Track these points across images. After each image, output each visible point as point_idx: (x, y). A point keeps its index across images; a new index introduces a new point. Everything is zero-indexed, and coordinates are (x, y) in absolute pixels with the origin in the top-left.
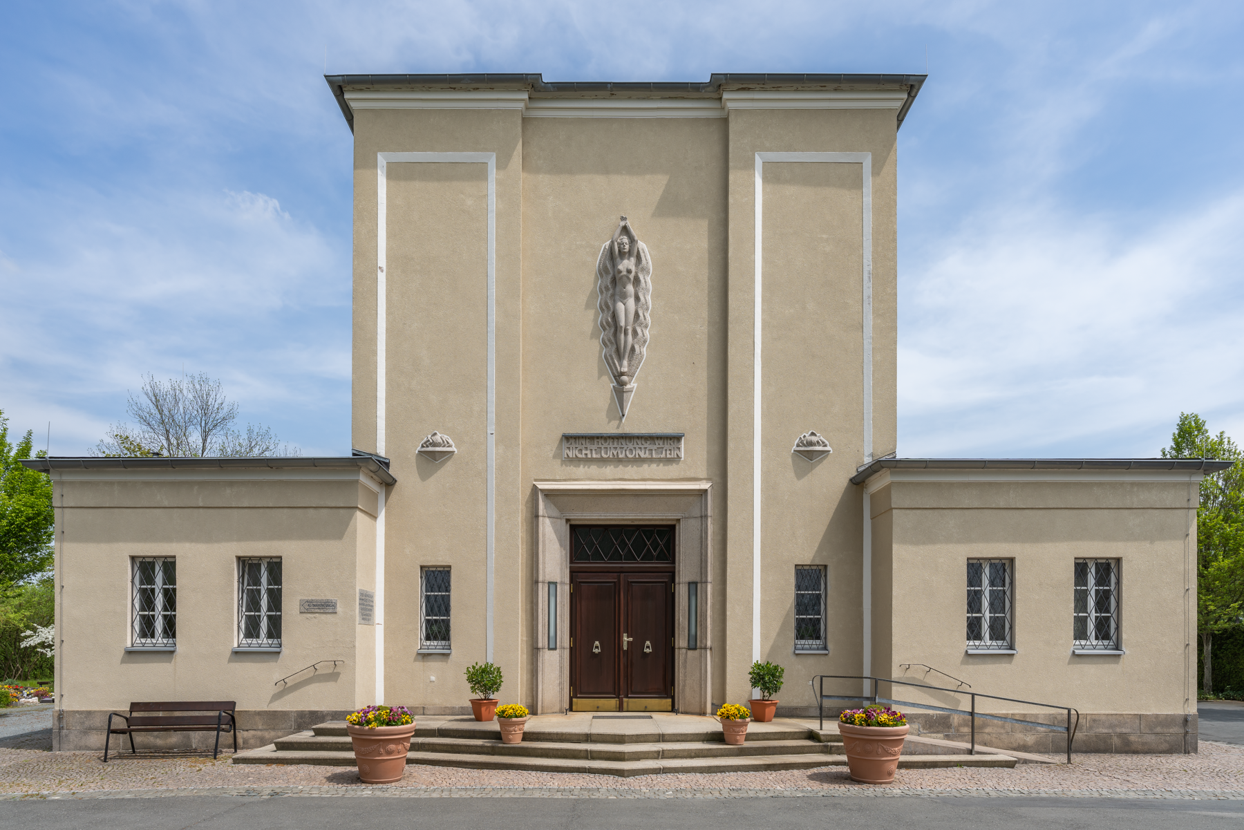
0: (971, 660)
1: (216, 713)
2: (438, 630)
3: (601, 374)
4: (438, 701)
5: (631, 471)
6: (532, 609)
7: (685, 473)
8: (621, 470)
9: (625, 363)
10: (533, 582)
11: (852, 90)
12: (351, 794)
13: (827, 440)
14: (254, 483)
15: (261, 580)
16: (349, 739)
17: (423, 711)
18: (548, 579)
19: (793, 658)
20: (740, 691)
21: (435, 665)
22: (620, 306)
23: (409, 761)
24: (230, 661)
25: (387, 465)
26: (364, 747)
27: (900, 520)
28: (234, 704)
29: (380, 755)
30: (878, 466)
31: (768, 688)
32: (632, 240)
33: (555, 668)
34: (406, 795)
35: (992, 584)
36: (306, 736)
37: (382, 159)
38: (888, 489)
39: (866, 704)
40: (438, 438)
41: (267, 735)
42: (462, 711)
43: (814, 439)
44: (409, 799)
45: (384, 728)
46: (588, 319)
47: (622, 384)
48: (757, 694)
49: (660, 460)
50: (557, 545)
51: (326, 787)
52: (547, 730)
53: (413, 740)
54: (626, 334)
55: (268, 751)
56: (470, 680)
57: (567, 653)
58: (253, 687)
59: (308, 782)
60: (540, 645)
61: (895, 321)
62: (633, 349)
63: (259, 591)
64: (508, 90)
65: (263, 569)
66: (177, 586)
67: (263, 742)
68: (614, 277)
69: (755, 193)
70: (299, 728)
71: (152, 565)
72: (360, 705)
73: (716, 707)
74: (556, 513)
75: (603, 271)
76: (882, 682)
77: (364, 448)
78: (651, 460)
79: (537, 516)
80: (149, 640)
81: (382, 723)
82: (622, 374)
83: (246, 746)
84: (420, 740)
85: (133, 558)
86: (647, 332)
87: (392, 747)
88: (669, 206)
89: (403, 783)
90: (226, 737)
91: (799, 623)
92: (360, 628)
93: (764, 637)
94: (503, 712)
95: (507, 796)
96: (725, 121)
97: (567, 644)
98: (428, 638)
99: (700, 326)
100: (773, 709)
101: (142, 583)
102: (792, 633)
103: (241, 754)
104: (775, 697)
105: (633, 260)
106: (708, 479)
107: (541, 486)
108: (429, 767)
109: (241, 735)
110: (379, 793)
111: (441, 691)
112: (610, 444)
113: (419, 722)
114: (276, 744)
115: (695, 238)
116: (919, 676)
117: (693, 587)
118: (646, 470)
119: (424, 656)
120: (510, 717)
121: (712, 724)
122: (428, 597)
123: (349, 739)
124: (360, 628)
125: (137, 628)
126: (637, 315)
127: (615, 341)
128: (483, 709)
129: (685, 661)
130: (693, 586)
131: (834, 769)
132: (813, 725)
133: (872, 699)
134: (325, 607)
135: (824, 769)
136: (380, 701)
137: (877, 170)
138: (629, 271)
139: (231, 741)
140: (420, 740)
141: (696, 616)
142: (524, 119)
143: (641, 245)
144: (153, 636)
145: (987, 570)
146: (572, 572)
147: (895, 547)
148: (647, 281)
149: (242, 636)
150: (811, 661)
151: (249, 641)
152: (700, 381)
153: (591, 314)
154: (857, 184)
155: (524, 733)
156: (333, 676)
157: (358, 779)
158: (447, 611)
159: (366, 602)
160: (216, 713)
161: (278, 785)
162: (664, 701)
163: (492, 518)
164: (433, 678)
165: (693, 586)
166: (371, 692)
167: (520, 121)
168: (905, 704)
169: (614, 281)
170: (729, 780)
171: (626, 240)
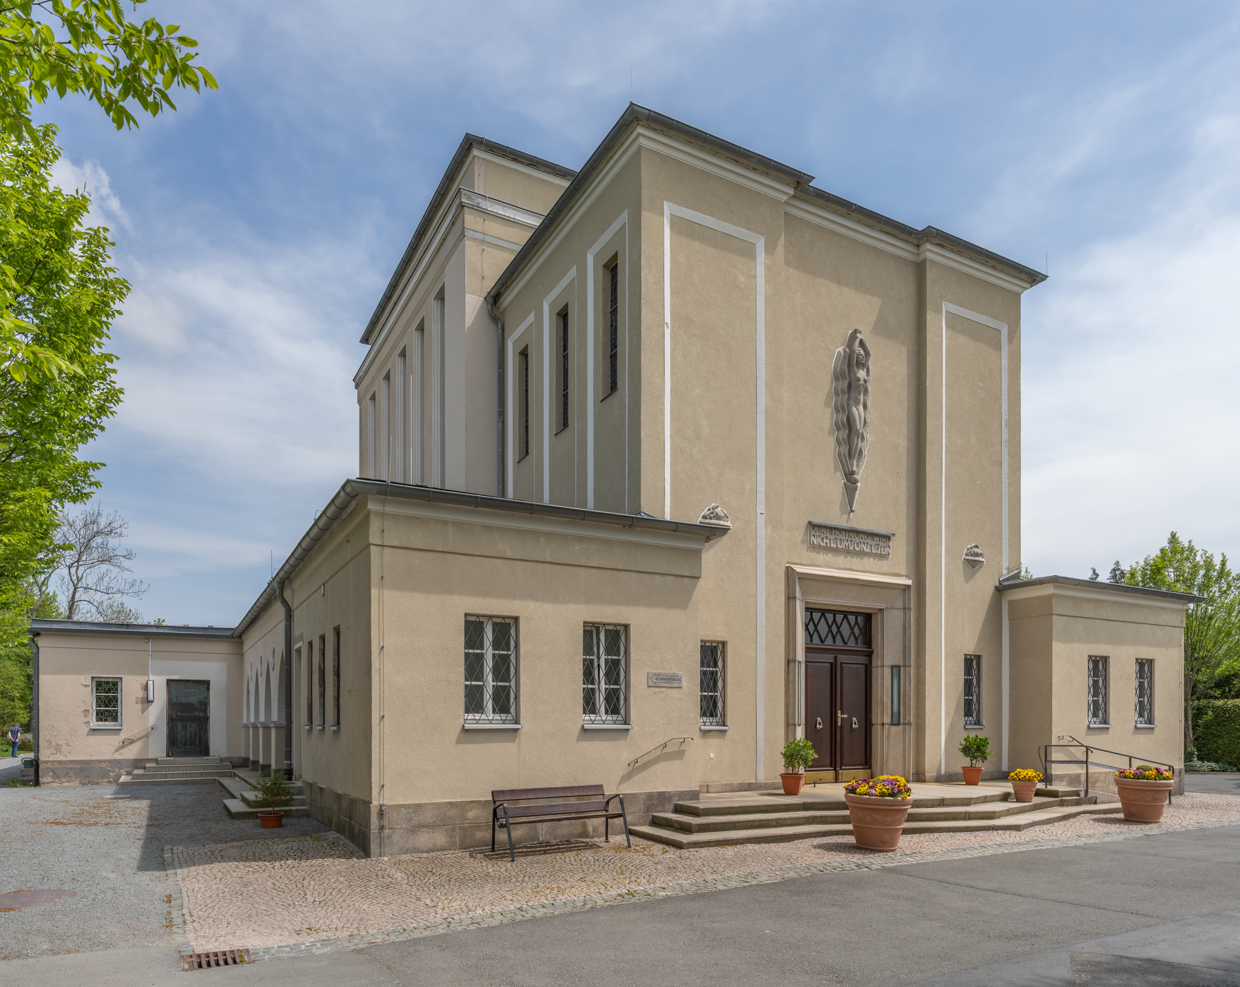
21: (714, 741)
46: (826, 417)
75: (837, 376)
78: (870, 555)
165: (895, 669)
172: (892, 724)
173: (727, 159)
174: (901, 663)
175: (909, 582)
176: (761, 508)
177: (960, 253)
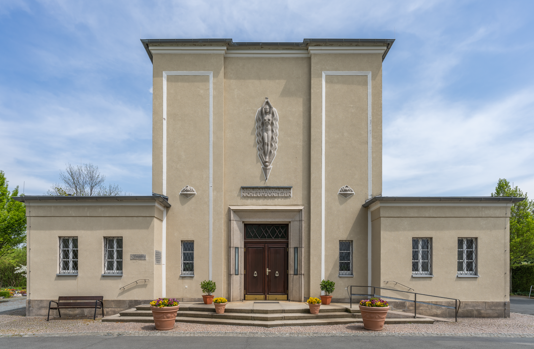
0: (414, 279)
1: (95, 301)
2: (189, 267)
3: (257, 162)
4: (189, 296)
5: (270, 201)
6: (228, 258)
7: (294, 202)
8: (265, 201)
9: (267, 157)
10: (229, 247)
11: (363, 46)
12: (152, 335)
13: (353, 189)
14: (111, 207)
15: (114, 246)
16: (151, 312)
17: (182, 300)
18: (235, 246)
19: (339, 279)
20: (316, 292)
21: (187, 281)
22: (265, 134)
23: (177, 321)
24: (101, 279)
25: (167, 199)
26: (158, 315)
27: (384, 222)
28: (102, 297)
29: (164, 318)
30: (375, 200)
31: (328, 291)
32: (270, 107)
33: (238, 282)
34: (175, 335)
35: (423, 248)
36: (133, 310)
37: (165, 74)
38: (379, 209)
39: (369, 297)
40: (188, 188)
41: (116, 310)
42: (199, 300)
43: (347, 189)
44: (177, 337)
45: (166, 307)
46: (252, 139)
47: (266, 166)
48: (323, 293)
49: (282, 197)
50: (239, 232)
51: (141, 332)
52: (235, 308)
53: (178, 312)
54: (268, 146)
55: (117, 316)
56: (202, 287)
57: (243, 276)
58: (111, 291)
59: (133, 330)
60: (232, 273)
61: (381, 140)
62: (271, 152)
63: (113, 251)
64: (218, 46)
65: (115, 242)
66: (78, 249)
67: (115, 313)
68: (263, 122)
69: (322, 88)
70: (130, 307)
71: (68, 240)
72: (156, 297)
73: (307, 298)
74: (238, 219)
75: (258, 120)
76: (376, 288)
77: (158, 192)
78: (278, 197)
79: (230, 220)
80: (66, 271)
81: (165, 305)
82: (266, 162)
83: (108, 314)
84: (181, 312)
85: (60, 237)
86: (277, 145)
87: (169, 315)
88: (286, 93)
89: (174, 330)
90: (99, 311)
91: (341, 264)
92: (156, 266)
93: (326, 270)
94: (216, 301)
95: (218, 335)
96: (309, 59)
97: (243, 273)
98: (184, 270)
99: (299, 142)
100: (330, 299)
101: (64, 247)
102: (338, 268)
103: (106, 318)
104: (331, 294)
105: (271, 115)
106: (302, 205)
107: (232, 208)
108: (185, 323)
109: (105, 310)
110: (164, 334)
111: (190, 291)
112: (261, 191)
113: (181, 305)
114: (120, 314)
115: (297, 107)
116: (392, 286)
117: (296, 249)
118: (276, 201)
119: (183, 278)
120: (220, 303)
121: (305, 306)
122: (184, 254)
123: (151, 312)
124: (156, 266)
125: (62, 266)
126: (272, 138)
127: (263, 148)
128: (208, 299)
129: (293, 280)
130: (296, 249)
131: (357, 324)
132: (348, 306)
133: (372, 295)
134: (141, 257)
135: (353, 324)
136: (164, 296)
137: (374, 77)
138: (269, 120)
139: (101, 312)
140: (181, 312)
141: (297, 261)
142: (225, 58)
143: (274, 109)
144: (68, 269)
145: (421, 243)
146: (245, 243)
147: (382, 232)
148: (277, 124)
149: (106, 269)
150: (346, 280)
151: (109, 271)
152: (299, 165)
153: (253, 137)
154: (366, 83)
155: (225, 309)
156: (145, 286)
157: (155, 328)
158: (192, 259)
159: (158, 256)
160: (95, 301)
161: (121, 331)
162: (284, 296)
163: (211, 221)
164: (186, 287)
165: (296, 249)
166: (160, 292)
167: (223, 59)
168: (387, 297)
169: (263, 124)
170: (312, 329)
171: (268, 107)
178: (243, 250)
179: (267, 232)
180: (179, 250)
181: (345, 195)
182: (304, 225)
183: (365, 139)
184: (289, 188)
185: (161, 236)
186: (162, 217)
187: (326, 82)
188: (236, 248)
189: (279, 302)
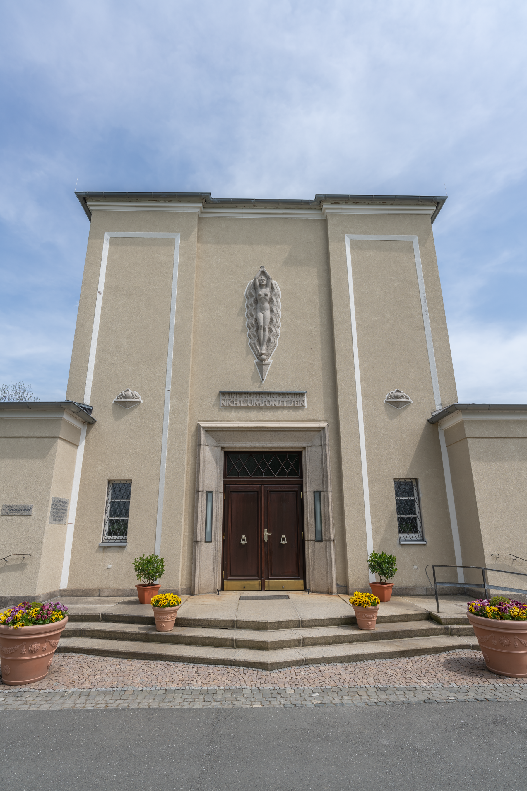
3: (247, 354)
5: (269, 415)
8: (261, 414)
9: (264, 348)
10: (195, 491)
11: (402, 205)
18: (207, 489)
22: (260, 315)
25: (91, 410)
32: (268, 278)
33: (210, 555)
37: (107, 236)
40: (129, 393)
43: (399, 394)
46: (240, 323)
47: (263, 360)
48: (374, 578)
49: (290, 408)
50: (214, 465)
54: (264, 330)
57: (220, 544)
60: (198, 539)
62: (269, 340)
68: (257, 297)
69: (346, 255)
74: (214, 443)
75: (249, 296)
78: (284, 408)
79: (199, 445)
82: (262, 354)
86: (279, 330)
88: (291, 261)
91: (401, 521)
93: (375, 532)
99: (315, 326)
100: (390, 591)
104: (389, 580)
106: (325, 421)
107: (203, 424)
112: (254, 398)
115: (310, 280)
117: (317, 495)
118: (280, 414)
122: (112, 503)
126: (272, 320)
127: (258, 335)
130: (317, 494)
132: (428, 605)
137: (422, 243)
138: (266, 295)
141: (321, 515)
142: (199, 218)
143: (274, 282)
146: (225, 484)
147: (473, 464)
148: (278, 302)
152: (317, 359)
153: (241, 319)
154: (411, 250)
164: (110, 566)
165: (317, 494)
167: (197, 218)
169: (256, 301)
171: (264, 278)
172: (316, 541)
173: (176, 202)
174: (321, 489)
175: (323, 424)
176: (169, 387)
177: (356, 204)
178: (221, 496)
179: (264, 465)
180: (103, 498)
181: (396, 404)
182: (330, 453)
183: (417, 325)
184: (302, 394)
185: (72, 472)
186: (78, 440)
187: (352, 248)
188: (209, 493)
189: (291, 594)
